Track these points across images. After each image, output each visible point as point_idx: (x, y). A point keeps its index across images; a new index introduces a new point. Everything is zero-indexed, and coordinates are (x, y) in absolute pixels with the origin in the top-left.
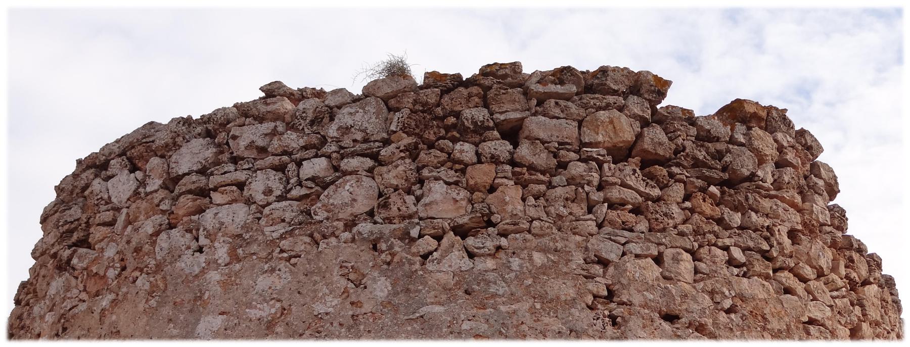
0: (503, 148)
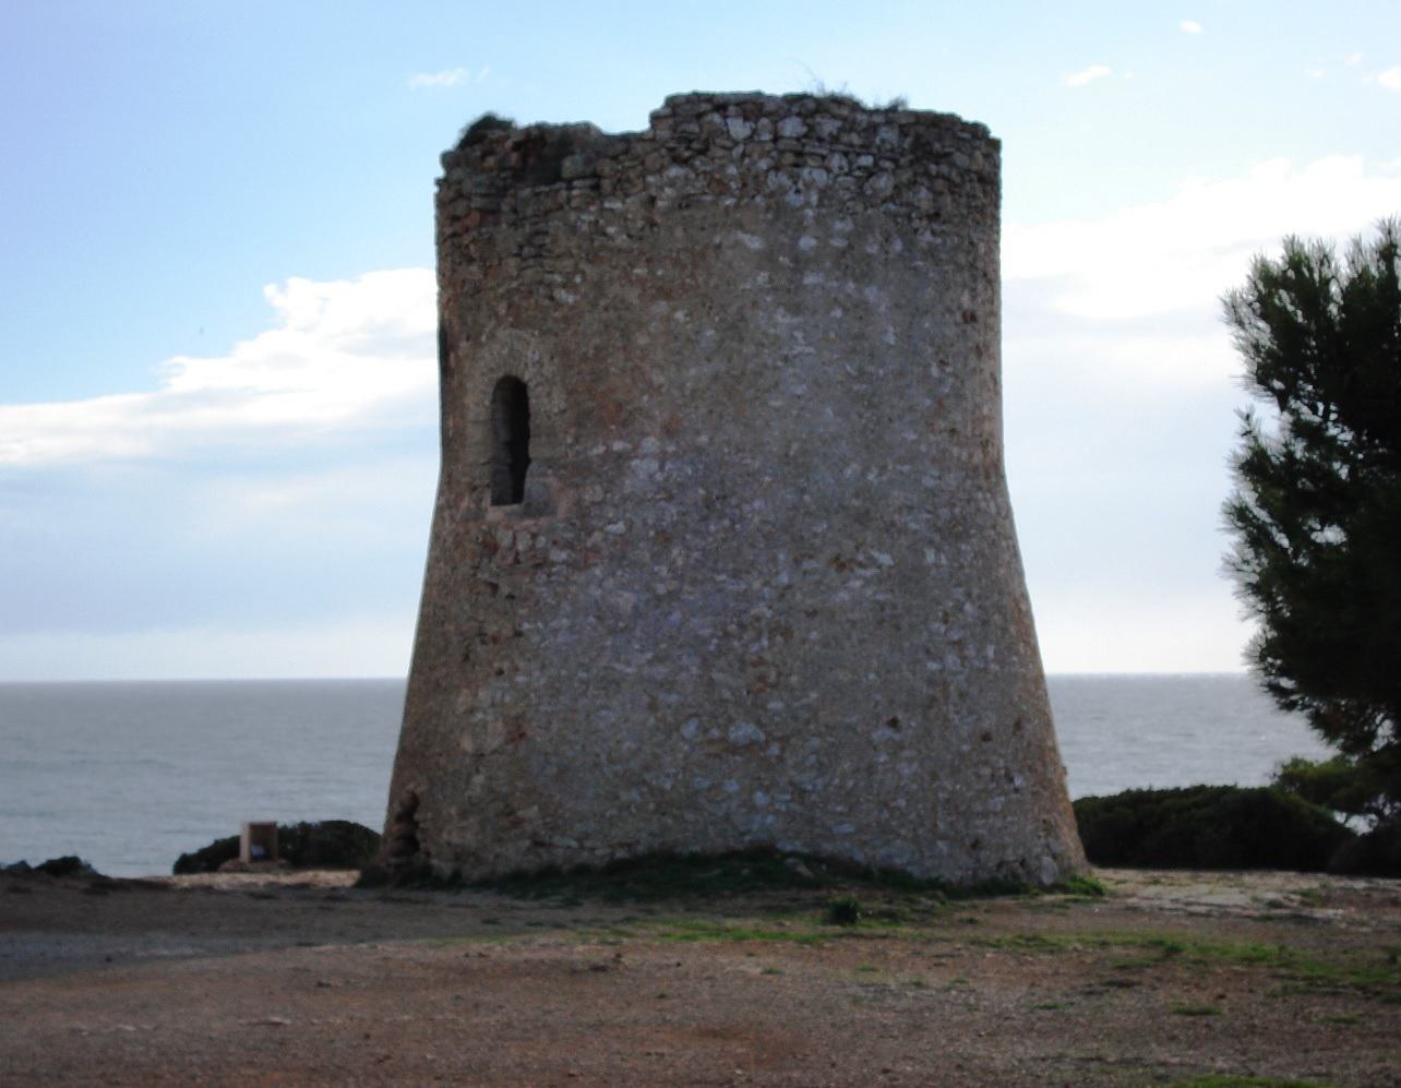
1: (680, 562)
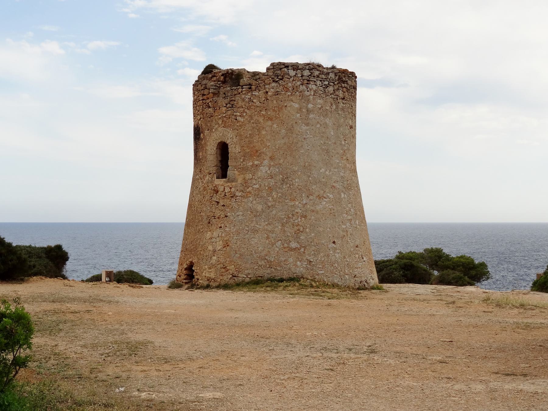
0: (346, 85)
1: (275, 196)
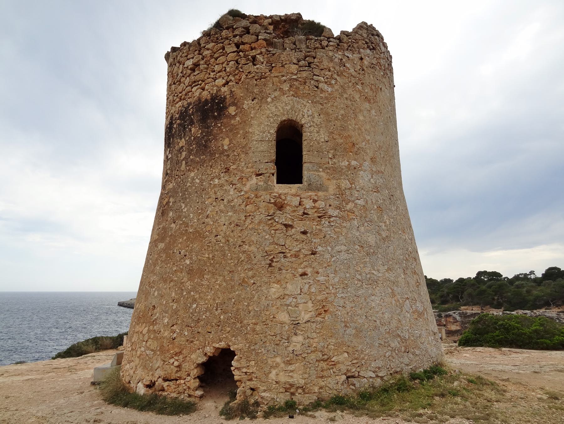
1: (388, 223)
